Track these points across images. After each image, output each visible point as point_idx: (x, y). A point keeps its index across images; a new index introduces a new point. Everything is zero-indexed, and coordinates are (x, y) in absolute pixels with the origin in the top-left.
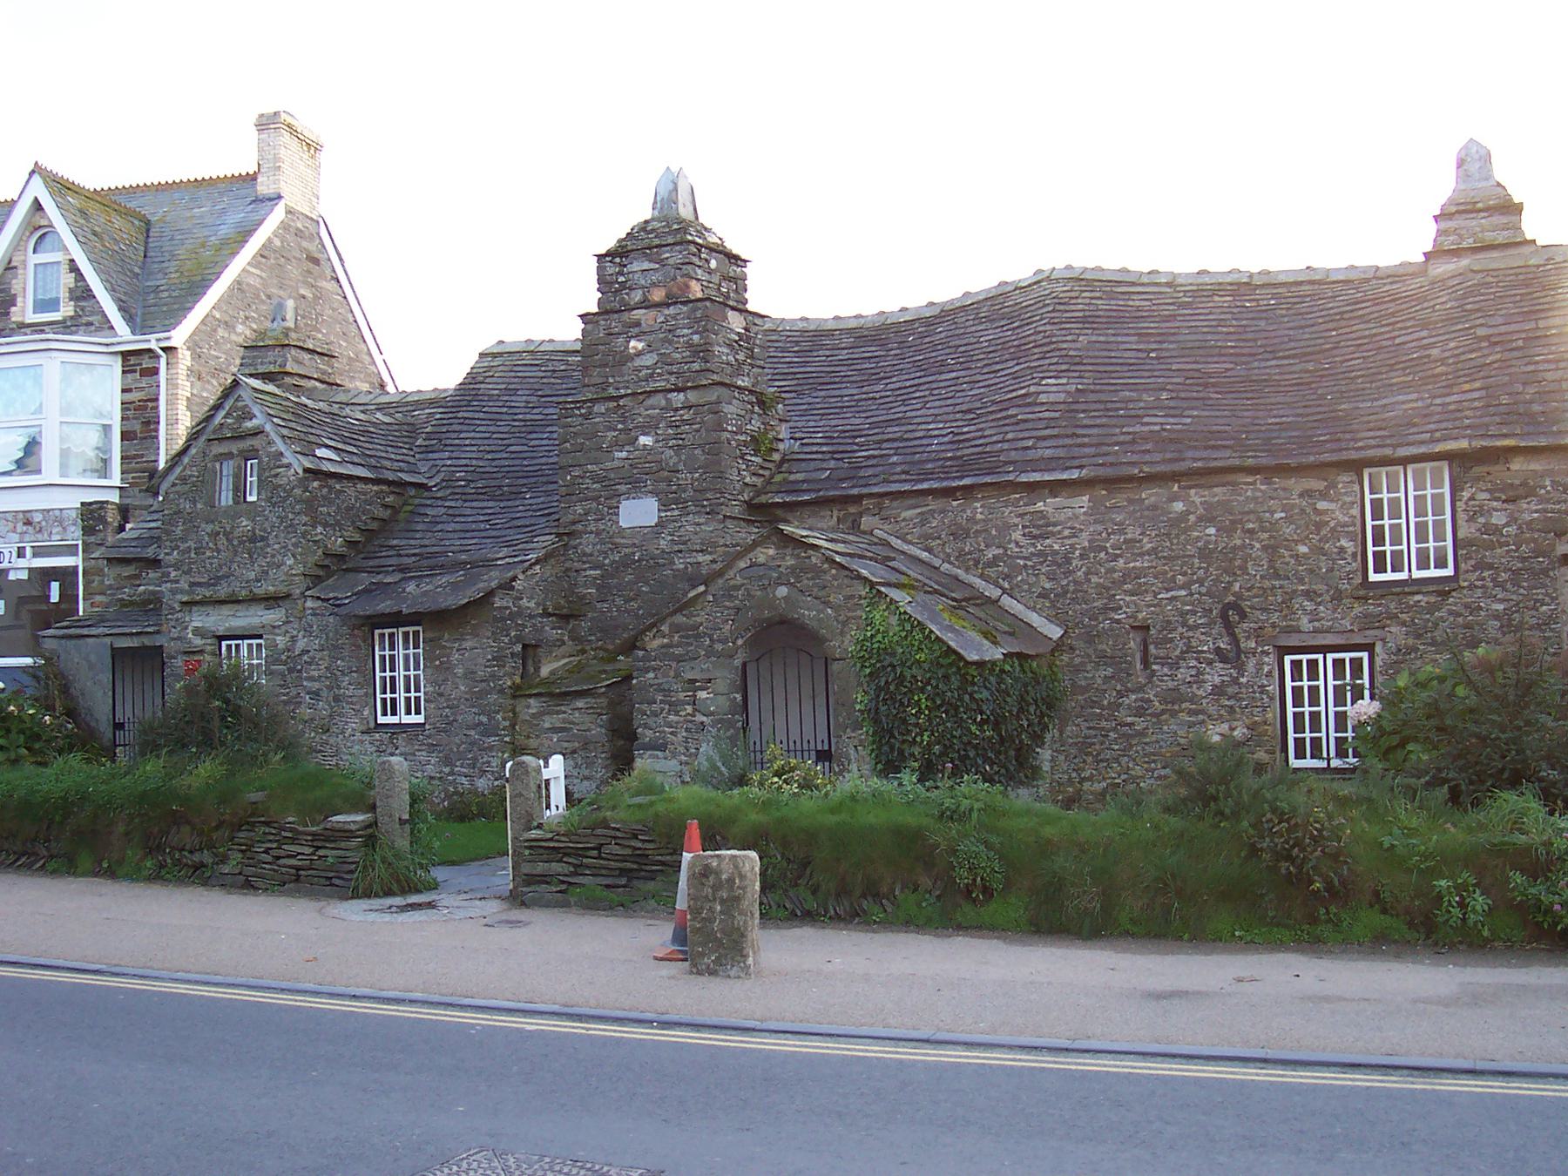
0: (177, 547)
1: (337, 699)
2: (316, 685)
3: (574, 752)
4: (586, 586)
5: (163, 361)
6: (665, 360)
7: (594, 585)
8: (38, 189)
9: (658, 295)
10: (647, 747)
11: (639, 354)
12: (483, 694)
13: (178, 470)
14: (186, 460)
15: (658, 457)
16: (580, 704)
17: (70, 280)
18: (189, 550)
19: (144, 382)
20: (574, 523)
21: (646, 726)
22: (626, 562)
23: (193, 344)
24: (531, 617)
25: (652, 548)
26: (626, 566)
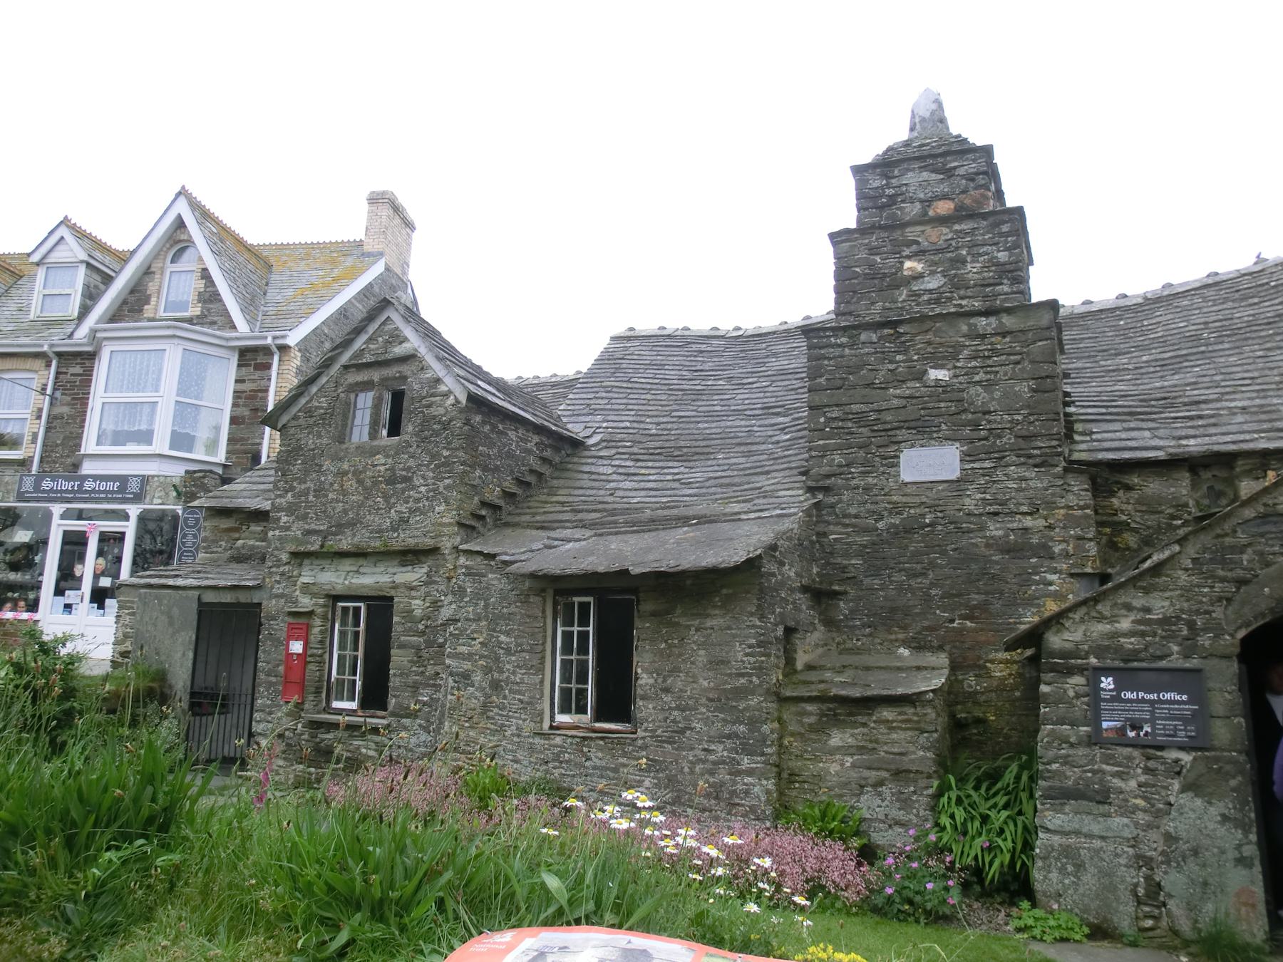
0: (292, 489)
1: (496, 686)
2: (467, 665)
3: (881, 783)
4: (846, 555)
5: (276, 358)
6: (957, 284)
7: (858, 555)
8: (182, 208)
9: (944, 208)
10: (1062, 796)
11: (918, 277)
12: (740, 693)
13: (303, 401)
14: (314, 389)
15: (956, 396)
16: (888, 714)
17: (201, 285)
18: (306, 493)
19: (258, 374)
20: (828, 476)
21: (1066, 761)
22: (908, 530)
23: (304, 345)
24: (792, 590)
25: (950, 511)
26: (909, 530)
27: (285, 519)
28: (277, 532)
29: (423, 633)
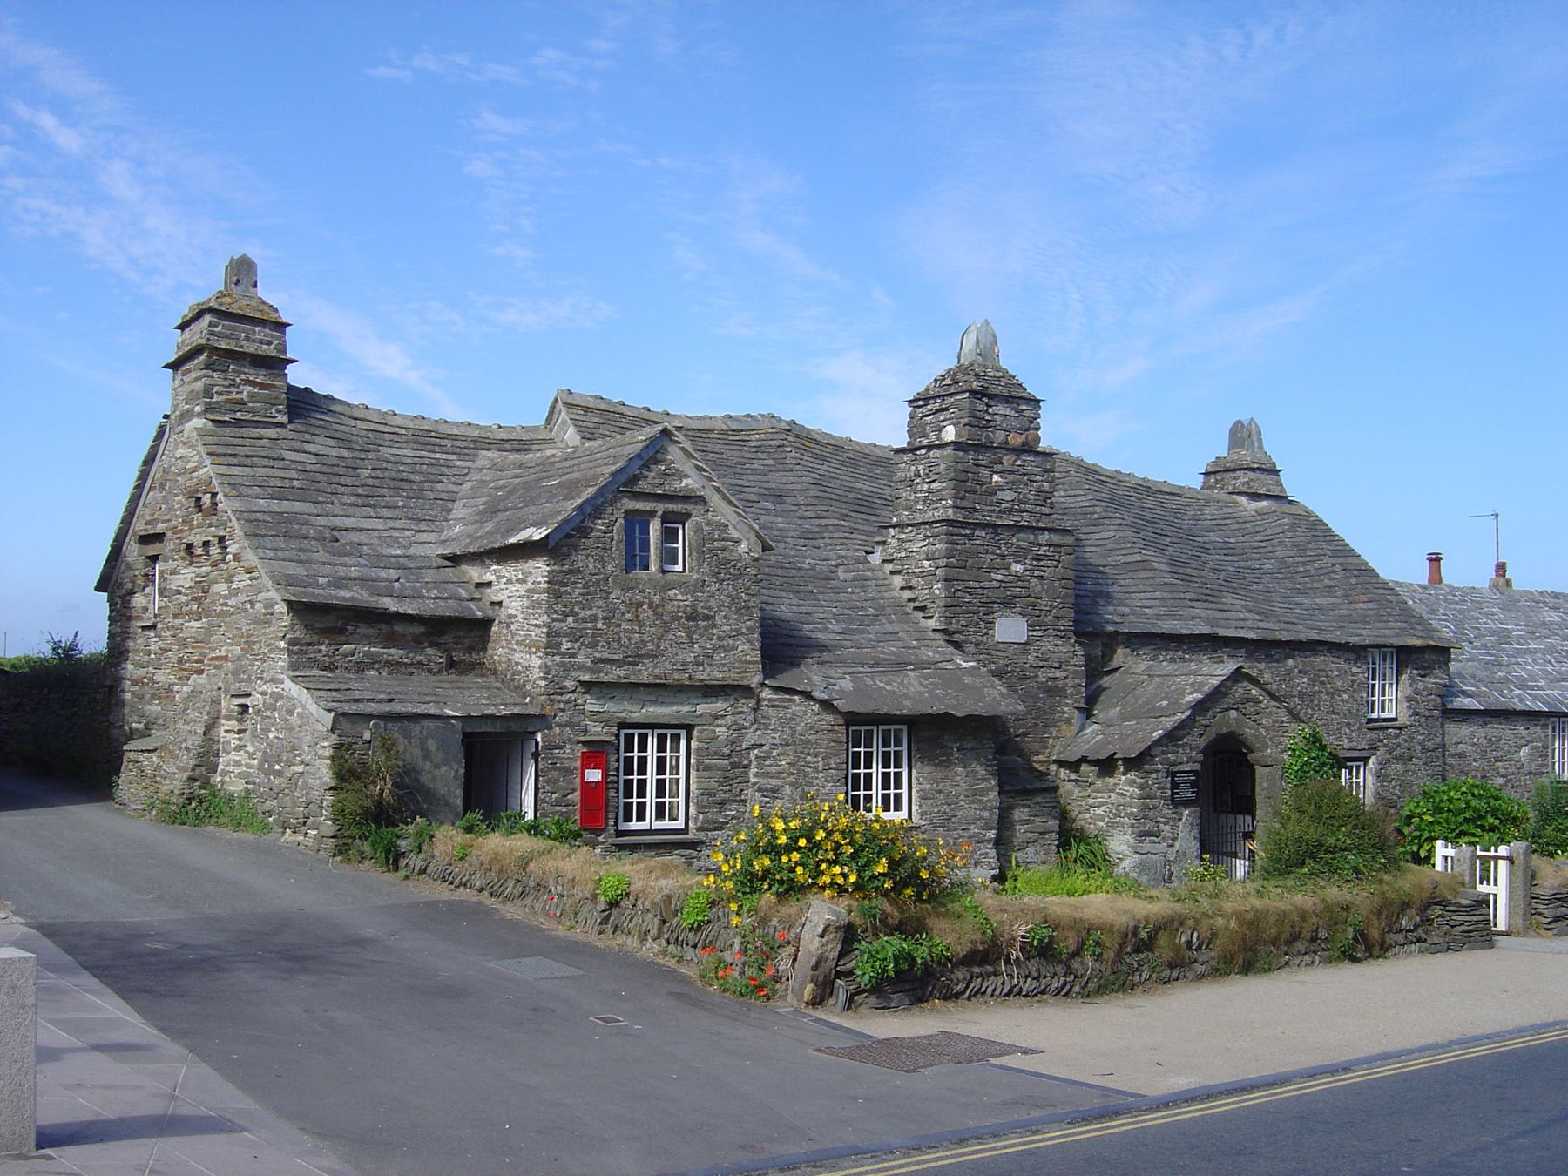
16: (1039, 799)
18: (595, 619)
27: (566, 646)
28: (557, 659)
29: (723, 757)
